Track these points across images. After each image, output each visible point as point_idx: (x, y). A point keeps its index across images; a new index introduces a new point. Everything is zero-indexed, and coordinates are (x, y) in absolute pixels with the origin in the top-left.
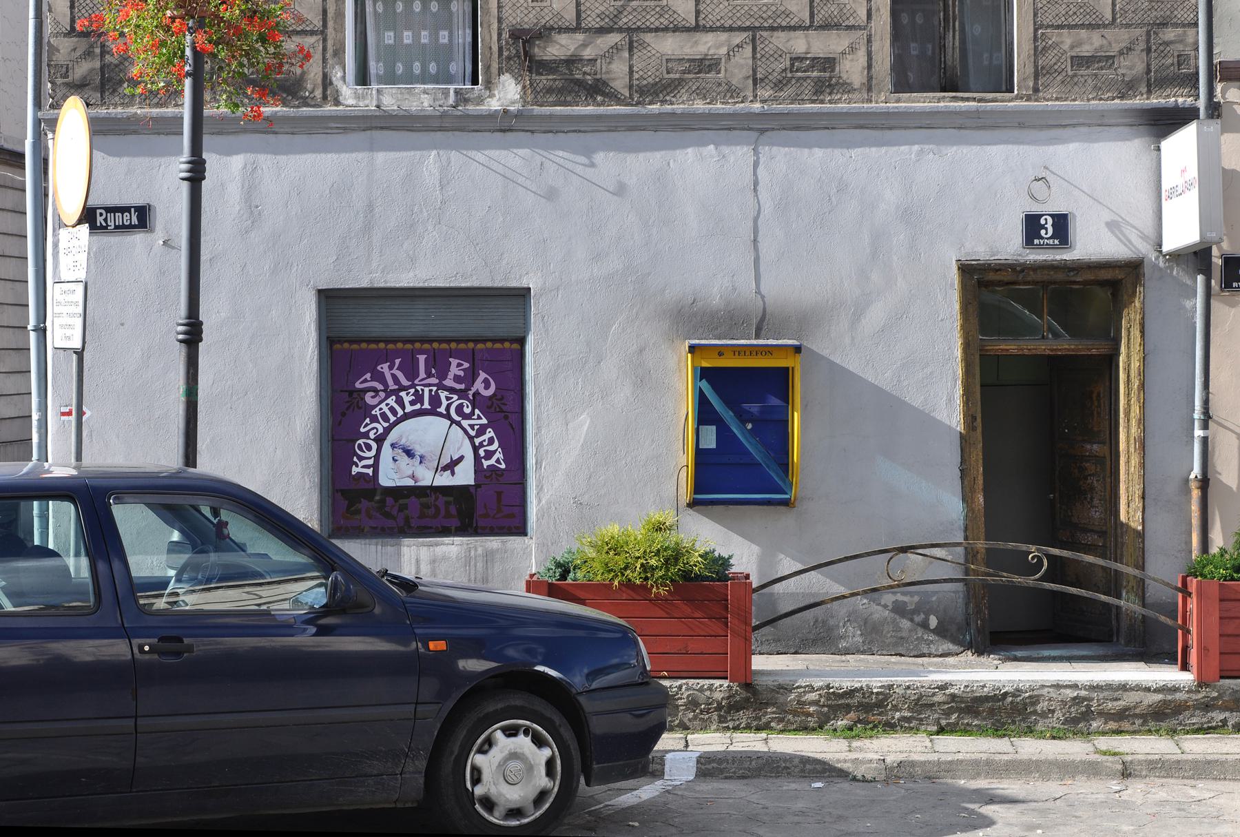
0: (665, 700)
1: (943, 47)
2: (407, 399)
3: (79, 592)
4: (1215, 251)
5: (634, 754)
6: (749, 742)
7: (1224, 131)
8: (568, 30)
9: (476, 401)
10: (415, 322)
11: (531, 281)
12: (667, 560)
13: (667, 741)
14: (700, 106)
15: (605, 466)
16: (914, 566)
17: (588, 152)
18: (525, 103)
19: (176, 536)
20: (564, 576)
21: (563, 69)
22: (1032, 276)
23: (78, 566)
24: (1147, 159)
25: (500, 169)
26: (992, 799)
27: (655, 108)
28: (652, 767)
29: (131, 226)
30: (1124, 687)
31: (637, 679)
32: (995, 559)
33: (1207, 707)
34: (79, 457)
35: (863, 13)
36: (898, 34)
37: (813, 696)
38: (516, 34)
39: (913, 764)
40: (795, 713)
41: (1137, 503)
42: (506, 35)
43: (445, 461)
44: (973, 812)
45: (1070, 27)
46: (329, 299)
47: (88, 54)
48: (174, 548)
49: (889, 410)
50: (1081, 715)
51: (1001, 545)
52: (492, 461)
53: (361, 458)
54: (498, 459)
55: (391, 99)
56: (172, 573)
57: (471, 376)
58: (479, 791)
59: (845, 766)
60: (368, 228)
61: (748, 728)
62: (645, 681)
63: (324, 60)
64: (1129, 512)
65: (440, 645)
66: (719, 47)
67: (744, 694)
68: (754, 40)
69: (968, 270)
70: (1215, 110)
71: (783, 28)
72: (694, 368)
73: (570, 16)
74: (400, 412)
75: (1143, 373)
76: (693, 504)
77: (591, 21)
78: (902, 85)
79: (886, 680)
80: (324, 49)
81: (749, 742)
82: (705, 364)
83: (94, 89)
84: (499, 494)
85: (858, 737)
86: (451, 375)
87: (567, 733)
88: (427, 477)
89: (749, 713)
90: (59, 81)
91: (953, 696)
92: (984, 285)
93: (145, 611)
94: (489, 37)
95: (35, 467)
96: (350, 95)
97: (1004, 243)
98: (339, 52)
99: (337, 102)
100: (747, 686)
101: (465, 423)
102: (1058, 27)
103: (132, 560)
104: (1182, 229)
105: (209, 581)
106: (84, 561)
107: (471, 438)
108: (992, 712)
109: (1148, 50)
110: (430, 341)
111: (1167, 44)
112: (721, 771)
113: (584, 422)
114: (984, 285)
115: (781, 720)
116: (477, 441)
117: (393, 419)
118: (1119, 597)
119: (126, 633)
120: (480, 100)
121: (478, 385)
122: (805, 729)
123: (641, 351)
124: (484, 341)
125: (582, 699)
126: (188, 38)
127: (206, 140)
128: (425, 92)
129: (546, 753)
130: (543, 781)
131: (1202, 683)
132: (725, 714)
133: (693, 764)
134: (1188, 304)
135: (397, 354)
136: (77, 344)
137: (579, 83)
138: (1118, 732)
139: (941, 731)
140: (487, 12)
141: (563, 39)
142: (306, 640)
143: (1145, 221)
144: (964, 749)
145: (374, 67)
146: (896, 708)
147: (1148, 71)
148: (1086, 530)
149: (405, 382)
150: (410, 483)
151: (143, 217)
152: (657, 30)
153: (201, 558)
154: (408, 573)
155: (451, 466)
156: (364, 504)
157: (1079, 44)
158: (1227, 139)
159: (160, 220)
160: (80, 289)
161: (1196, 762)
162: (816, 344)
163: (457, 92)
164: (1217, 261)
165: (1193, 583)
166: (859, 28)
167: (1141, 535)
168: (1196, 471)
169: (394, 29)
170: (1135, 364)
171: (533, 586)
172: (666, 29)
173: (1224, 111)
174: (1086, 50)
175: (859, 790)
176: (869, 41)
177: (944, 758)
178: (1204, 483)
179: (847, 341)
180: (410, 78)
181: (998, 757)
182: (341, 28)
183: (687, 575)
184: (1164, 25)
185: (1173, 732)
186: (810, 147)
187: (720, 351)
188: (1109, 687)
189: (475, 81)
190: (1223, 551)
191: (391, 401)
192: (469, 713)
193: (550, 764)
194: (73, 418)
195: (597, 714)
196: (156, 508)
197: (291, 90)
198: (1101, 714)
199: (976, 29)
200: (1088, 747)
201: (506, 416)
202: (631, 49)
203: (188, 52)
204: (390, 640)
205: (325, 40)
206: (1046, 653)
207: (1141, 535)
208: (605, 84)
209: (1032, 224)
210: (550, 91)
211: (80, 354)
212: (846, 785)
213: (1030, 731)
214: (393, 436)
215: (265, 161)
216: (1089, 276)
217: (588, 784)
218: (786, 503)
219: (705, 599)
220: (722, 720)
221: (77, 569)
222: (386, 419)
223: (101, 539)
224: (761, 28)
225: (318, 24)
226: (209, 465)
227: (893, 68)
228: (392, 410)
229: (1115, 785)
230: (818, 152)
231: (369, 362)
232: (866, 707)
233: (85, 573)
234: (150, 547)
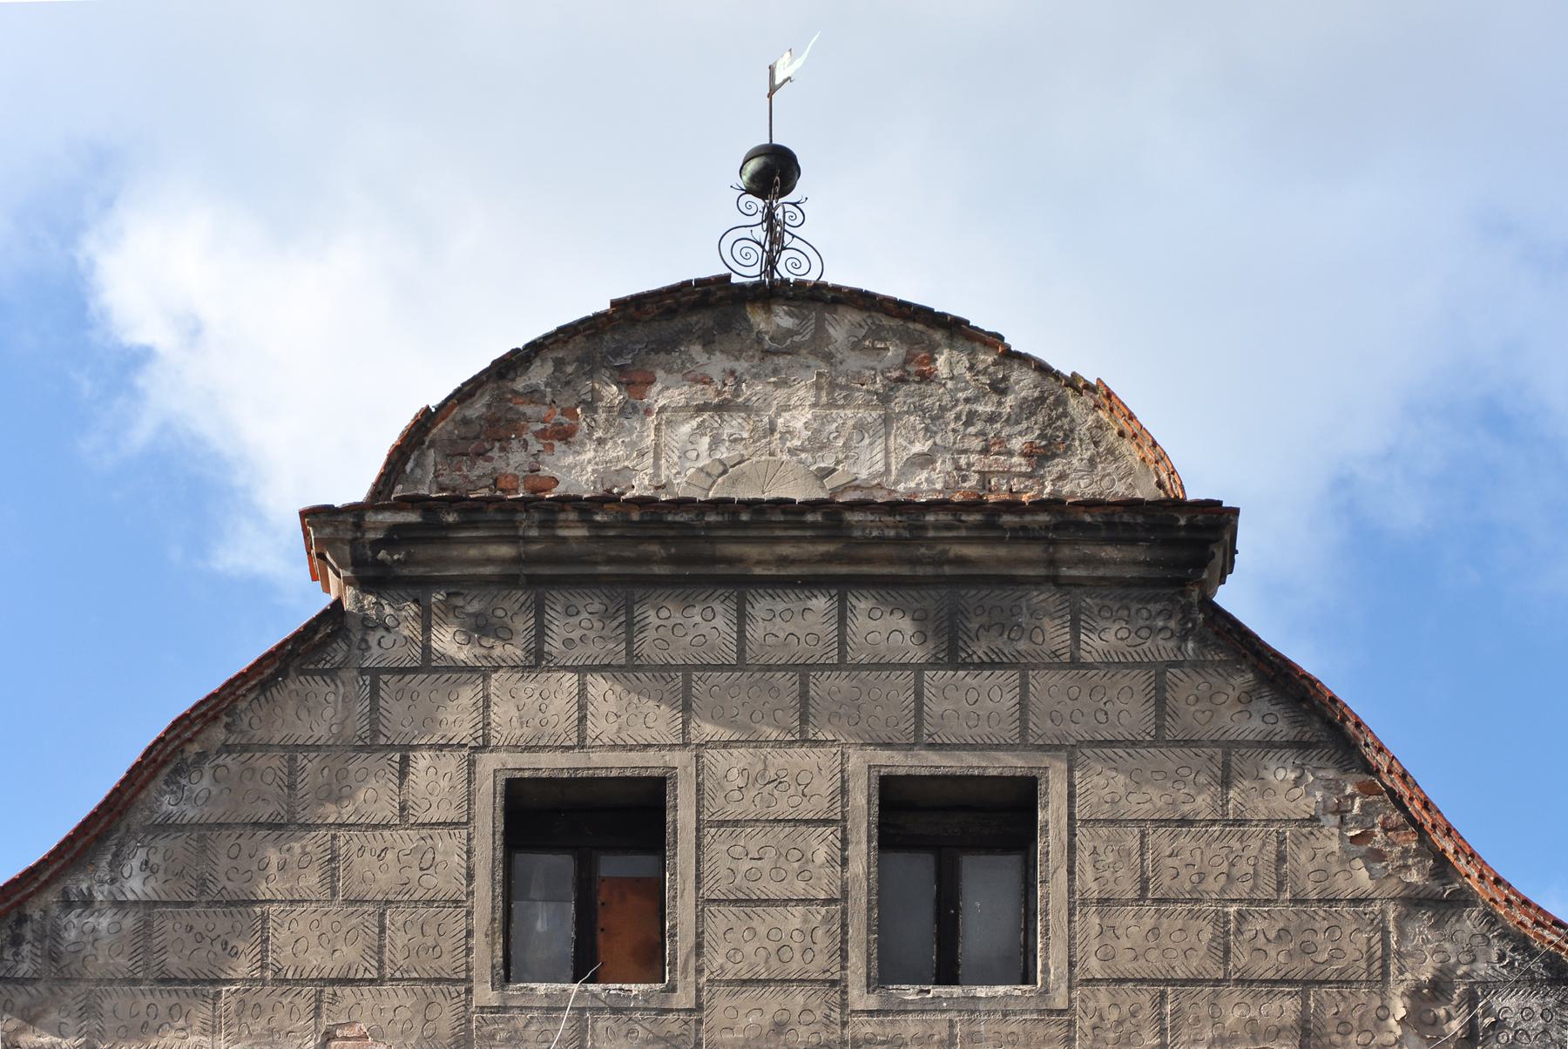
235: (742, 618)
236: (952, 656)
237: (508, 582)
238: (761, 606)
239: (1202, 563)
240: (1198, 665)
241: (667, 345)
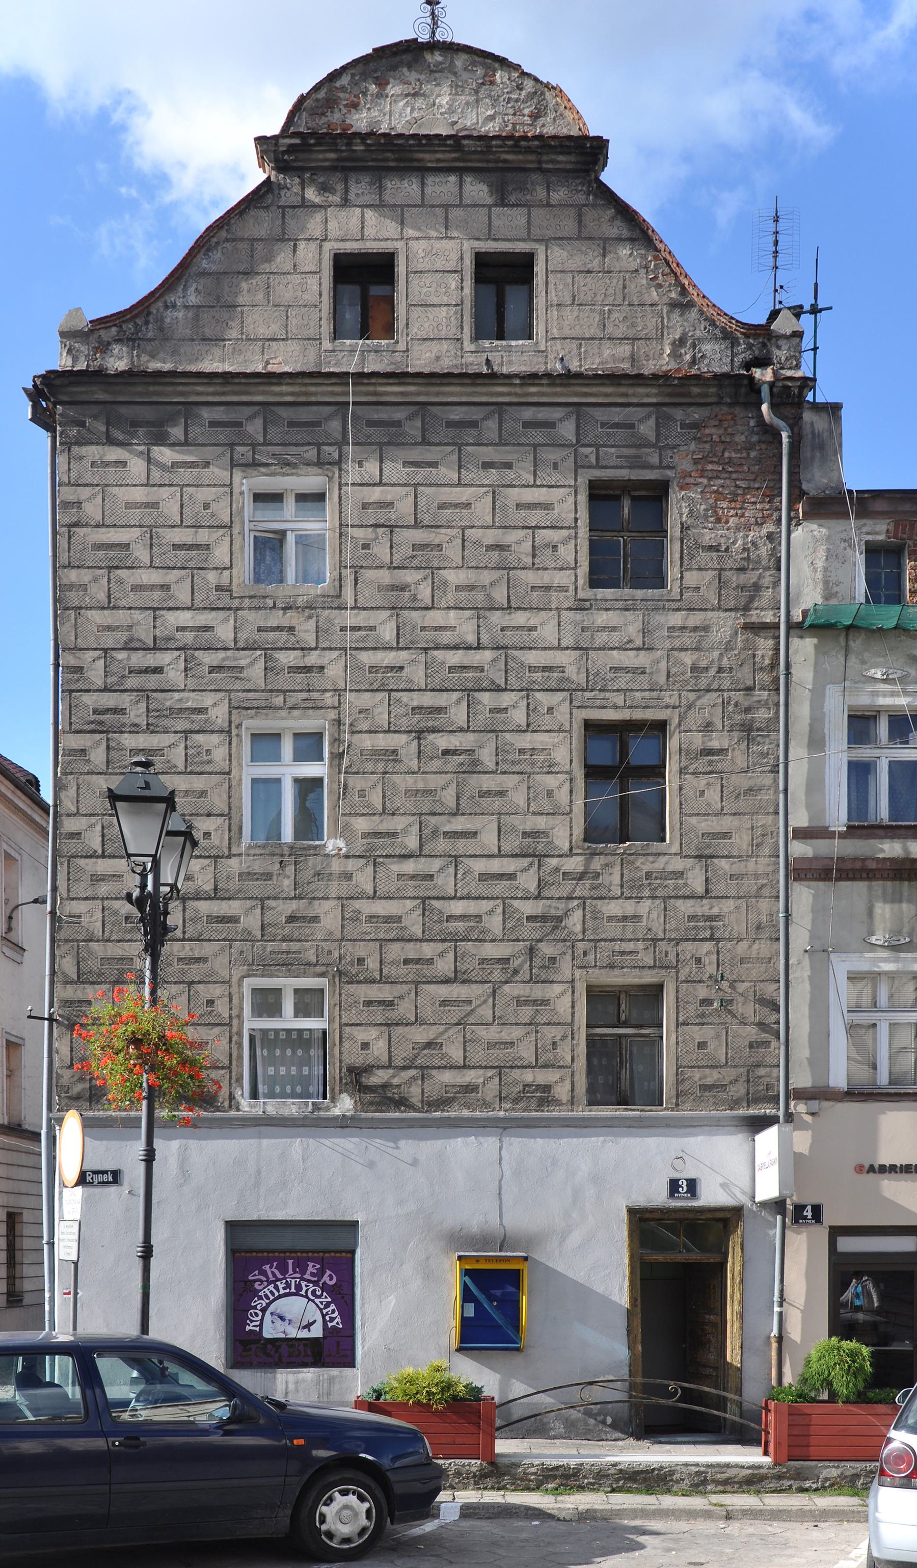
0: (441, 1473)
1: (619, 1079)
2: (281, 1285)
3: (73, 1407)
4: (788, 1201)
5: (423, 1504)
6: (492, 1497)
7: (795, 1129)
8: (383, 1067)
9: (324, 1288)
10: (287, 1241)
11: (360, 1217)
12: (443, 1389)
13: (443, 1496)
14: (466, 1113)
15: (405, 1330)
16: (598, 1394)
17: (395, 1140)
18: (356, 1111)
19: (135, 1374)
20: (378, 1398)
21: (380, 1091)
22: (674, 1216)
23: (73, 1392)
24: (746, 1147)
25: (341, 1150)
26: (644, 1532)
27: (438, 1114)
28: (433, 1512)
29: (108, 1182)
30: (728, 1466)
31: (424, 1461)
32: (647, 1389)
33: (780, 1477)
34: (75, 1328)
35: (569, 1059)
36: (591, 1070)
37: (533, 1470)
38: (351, 1070)
39: (595, 1511)
40: (522, 1480)
41: (738, 1351)
42: (344, 1070)
43: (305, 1323)
44: (632, 1540)
45: (699, 1067)
46: (231, 1226)
47: (81, 1079)
48: (134, 1381)
49: (583, 1293)
50: (702, 1481)
51: (652, 1381)
52: (334, 1323)
53: (252, 1321)
54: (337, 1322)
55: (272, 1107)
56: (133, 1396)
57: (321, 1273)
58: (324, 1527)
59: (553, 1512)
60: (257, 1185)
61: (493, 1488)
62: (428, 1463)
63: (230, 1084)
64: (733, 1356)
65: (301, 1442)
66: (479, 1077)
67: (490, 1468)
68: (500, 1074)
69: (632, 1211)
70: (790, 1117)
71: (518, 1067)
72: (461, 1270)
73: (385, 1059)
74: (277, 1294)
75: (742, 1273)
76: (459, 1350)
77: (398, 1062)
78: (591, 1103)
79: (579, 1461)
80: (230, 1078)
81: (492, 1497)
82: (467, 1267)
83: (86, 1100)
84: (338, 1343)
85: (561, 1494)
86: (308, 1272)
87: (379, 1494)
88: (293, 1333)
89: (493, 1480)
90: (63, 1095)
91: (621, 1470)
92: (645, 1224)
93: (115, 1421)
94: (334, 1071)
95: (49, 1334)
96: (246, 1105)
97: (656, 1195)
98: (240, 1079)
99: (238, 1110)
100: (492, 1463)
101: (317, 1301)
102: (692, 1067)
103: (107, 1390)
104: (768, 1187)
105: (156, 1402)
106: (78, 1389)
107: (321, 1310)
108: (645, 1479)
109: (748, 1081)
110: (296, 1252)
111: (760, 1077)
112: (476, 1514)
113: (392, 1301)
114: (645, 1224)
115: (513, 1484)
116: (325, 1311)
117: (272, 1298)
118: (725, 1412)
119: (104, 1434)
120: (328, 1109)
121: (326, 1278)
122: (528, 1489)
123: (428, 1258)
124: (329, 1252)
125: (388, 1473)
126: (145, 1076)
127: (156, 1131)
128: (293, 1104)
129: (366, 1505)
130: (364, 1522)
131: (776, 1463)
132: (479, 1480)
133: (458, 1510)
134: (771, 1233)
135: (275, 1259)
136: (75, 1259)
137: (391, 1099)
138: (724, 1492)
139: (613, 1491)
140: (332, 1056)
141: (380, 1073)
142: (216, 1439)
143: (745, 1184)
144: (627, 1502)
145: (261, 1088)
146: (585, 1477)
147: (748, 1093)
148: (705, 1366)
149: (280, 1276)
150: (283, 1336)
151: (116, 1177)
152: (439, 1068)
153: (151, 1387)
154: (279, 1397)
155: (308, 1326)
156: (253, 1346)
157: (705, 1077)
158: (796, 1134)
159: (126, 1178)
160: (76, 1225)
161: (772, 1511)
162: (535, 1255)
163: (313, 1104)
164: (790, 1207)
165: (772, 1405)
166: (567, 1067)
167: (740, 1370)
168: (775, 1332)
169: (274, 1066)
170: (738, 1268)
171: (359, 1404)
172: (445, 1067)
173: (795, 1118)
174: (709, 1081)
175: (562, 1527)
176: (572, 1075)
177: (614, 1507)
178: (780, 1339)
179: (557, 1253)
180: (284, 1095)
181: (648, 1507)
182: (240, 1065)
183: (455, 1398)
184: (758, 1066)
185: (758, 1492)
186: (534, 1137)
187: (477, 1259)
188: (719, 1465)
189: (325, 1098)
190: (791, 1386)
191: (271, 1287)
192: (319, 1482)
193: (368, 1512)
194: (71, 1296)
195: (398, 1482)
196: (125, 1360)
197: (207, 1100)
198: (713, 1481)
199: (640, 1068)
200: (705, 1501)
201: (343, 1296)
202: (423, 1079)
203: (145, 1085)
204: (269, 1438)
205: (231, 1072)
206: (679, 1439)
207: (740, 1370)
208: (407, 1100)
209: (674, 1185)
210: (372, 1103)
211: (76, 1264)
212: (553, 1523)
213: (668, 1491)
214: (272, 1308)
215: (193, 1144)
216: (710, 1216)
217: (392, 1523)
218: (518, 1349)
219: (468, 1415)
220: (476, 1483)
221: (73, 1394)
222: (268, 1298)
223: (89, 1377)
224: (504, 1067)
225: (227, 1063)
226: (156, 1333)
227: (588, 1091)
228: (271, 1292)
229: (721, 1524)
230: (540, 1141)
231: (258, 1265)
232: (566, 1477)
233: (78, 1395)
234: (120, 1382)
235: (423, 185)
236: (502, 202)
237: (334, 169)
238: (430, 180)
239: (595, 162)
240: (594, 206)
241: (394, 68)
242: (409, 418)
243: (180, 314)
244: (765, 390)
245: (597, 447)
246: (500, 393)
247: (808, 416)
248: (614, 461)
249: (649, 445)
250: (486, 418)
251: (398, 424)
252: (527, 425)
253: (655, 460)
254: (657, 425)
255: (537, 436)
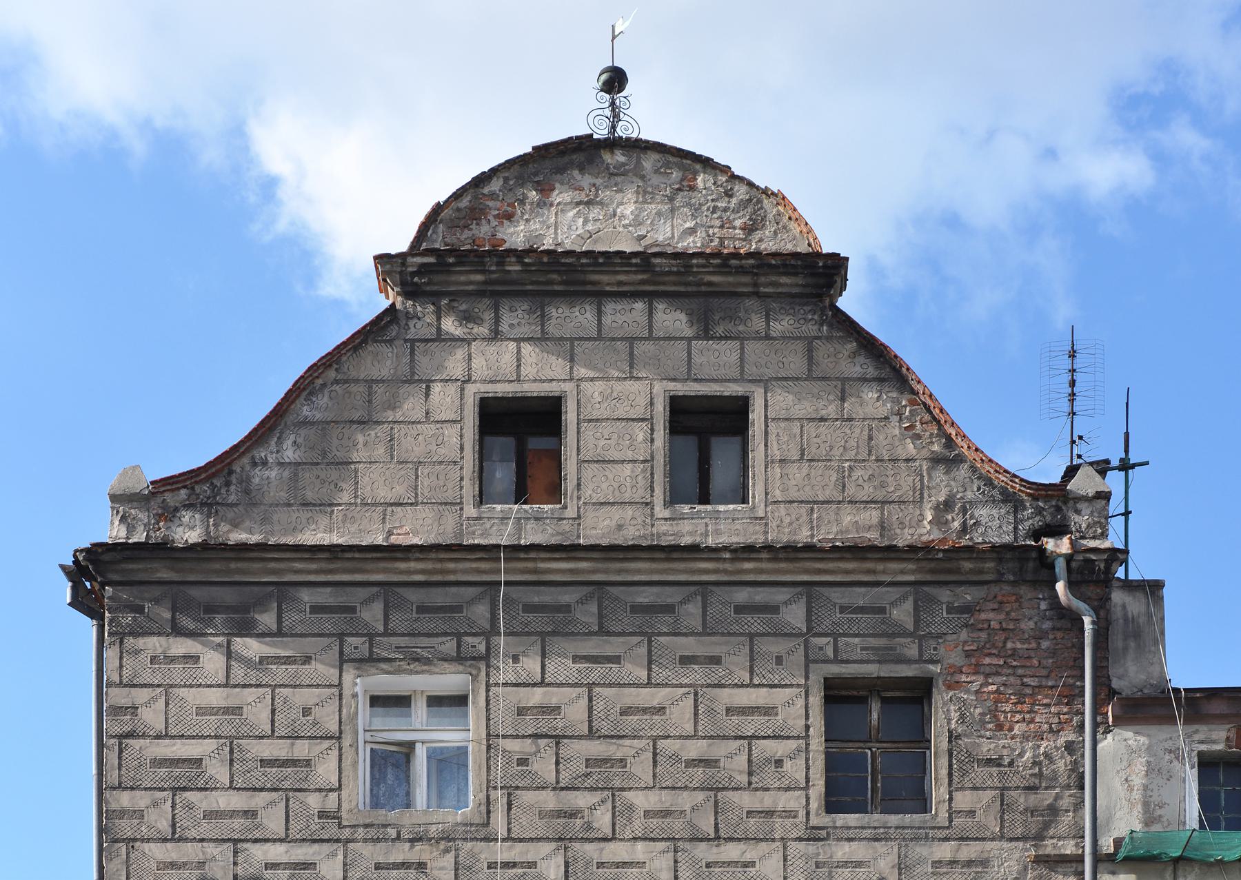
235: (600, 313)
236: (706, 333)
237: (480, 294)
238: (609, 306)
240: (829, 338)
241: (561, 170)
242: (582, 601)
243: (273, 474)
244: (1060, 566)
245: (835, 636)
246: (705, 570)
247: (1118, 597)
248: (858, 654)
249: (905, 634)
250: (685, 601)
251: (566, 608)
252: (740, 609)
253: (913, 652)
254: (916, 608)
255: (755, 623)
